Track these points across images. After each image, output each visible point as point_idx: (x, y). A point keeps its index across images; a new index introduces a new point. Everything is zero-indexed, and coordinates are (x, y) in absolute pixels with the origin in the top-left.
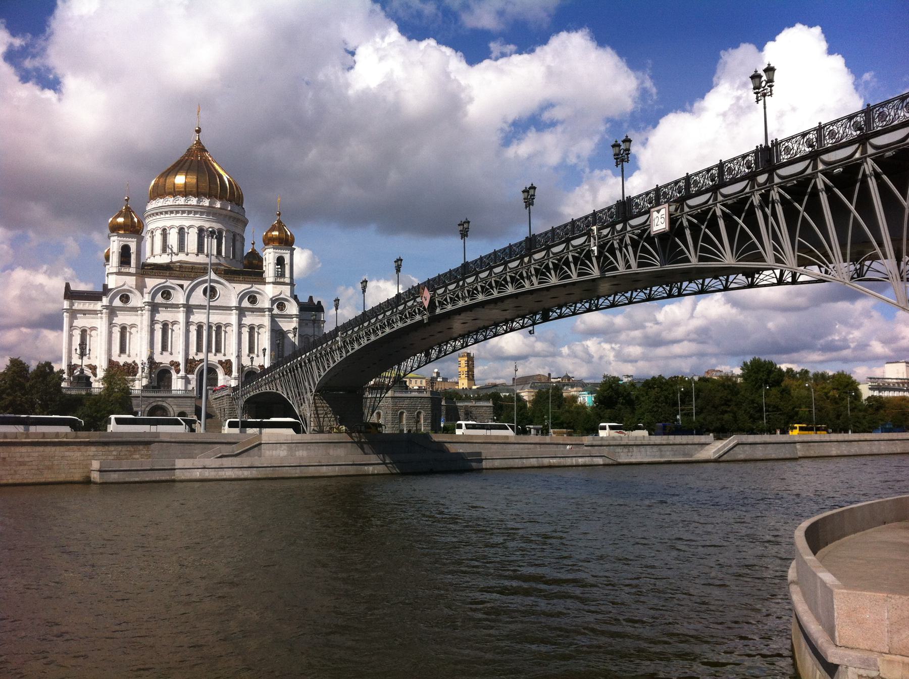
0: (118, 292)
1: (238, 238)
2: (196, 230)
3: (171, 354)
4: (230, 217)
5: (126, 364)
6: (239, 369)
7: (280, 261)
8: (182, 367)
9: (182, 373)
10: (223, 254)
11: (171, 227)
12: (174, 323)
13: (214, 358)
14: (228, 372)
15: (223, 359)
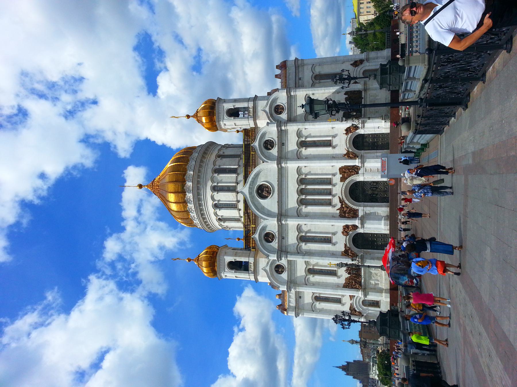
0: (272, 275)
1: (221, 153)
2: (215, 193)
3: (334, 234)
4: (202, 161)
5: (349, 271)
6: (351, 158)
7: (234, 113)
8: (350, 222)
9: (357, 222)
10: (236, 167)
11: (216, 214)
12: (299, 228)
13: (339, 188)
14: (355, 170)
15: (339, 176)
